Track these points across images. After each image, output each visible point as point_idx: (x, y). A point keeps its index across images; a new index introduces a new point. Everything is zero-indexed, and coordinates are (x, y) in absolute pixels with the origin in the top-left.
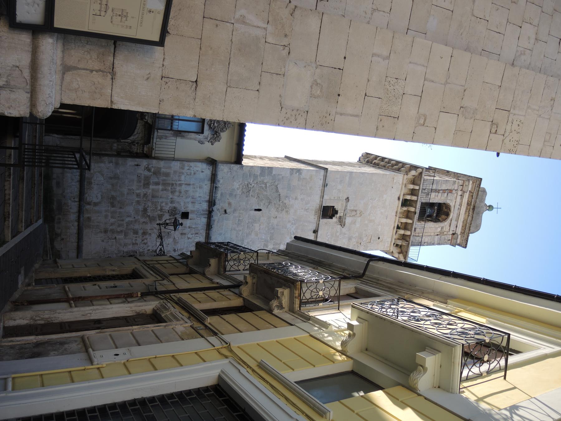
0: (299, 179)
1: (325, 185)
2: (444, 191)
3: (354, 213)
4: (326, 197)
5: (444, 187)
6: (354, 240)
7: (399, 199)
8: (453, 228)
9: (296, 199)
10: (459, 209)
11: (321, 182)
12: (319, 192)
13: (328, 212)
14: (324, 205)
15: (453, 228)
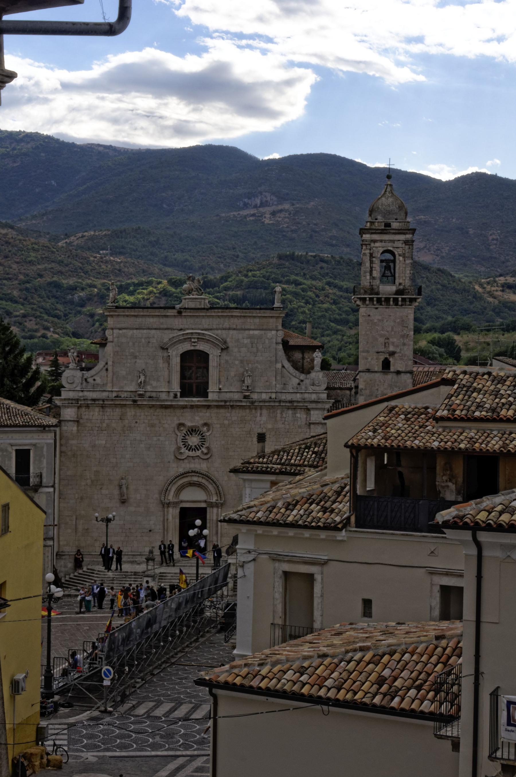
0: (366, 389)
1: (368, 371)
2: (371, 262)
3: (387, 345)
4: (376, 369)
5: (368, 264)
6: (405, 341)
7: (377, 308)
8: (400, 244)
9: (377, 390)
10: (385, 241)
11: (367, 374)
12: (373, 374)
13: (386, 365)
14: (380, 369)
15: (400, 244)
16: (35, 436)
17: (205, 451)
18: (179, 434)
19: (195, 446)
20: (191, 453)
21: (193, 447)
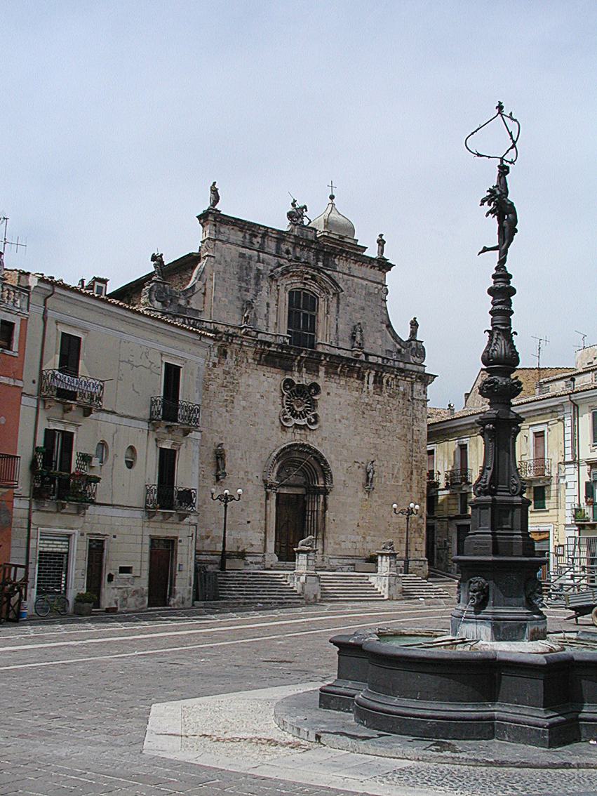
16: (187, 347)
17: (313, 420)
18: (286, 393)
19: (301, 412)
20: (298, 421)
21: (298, 413)
